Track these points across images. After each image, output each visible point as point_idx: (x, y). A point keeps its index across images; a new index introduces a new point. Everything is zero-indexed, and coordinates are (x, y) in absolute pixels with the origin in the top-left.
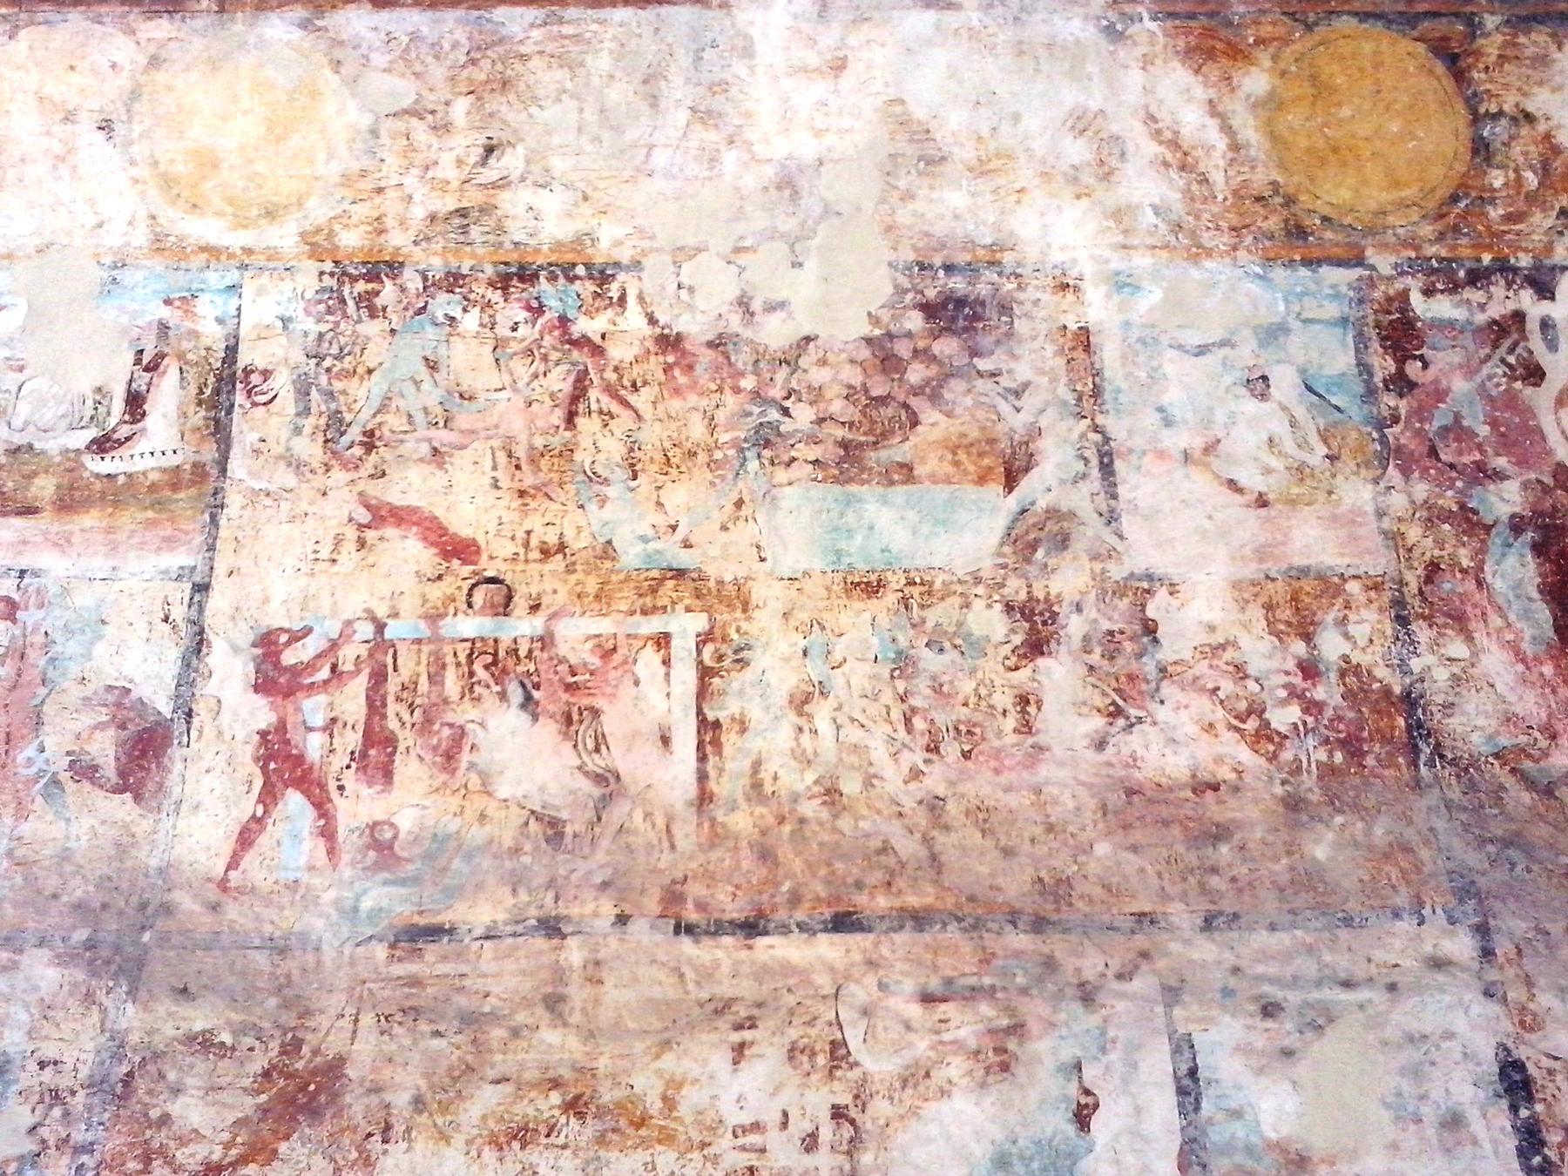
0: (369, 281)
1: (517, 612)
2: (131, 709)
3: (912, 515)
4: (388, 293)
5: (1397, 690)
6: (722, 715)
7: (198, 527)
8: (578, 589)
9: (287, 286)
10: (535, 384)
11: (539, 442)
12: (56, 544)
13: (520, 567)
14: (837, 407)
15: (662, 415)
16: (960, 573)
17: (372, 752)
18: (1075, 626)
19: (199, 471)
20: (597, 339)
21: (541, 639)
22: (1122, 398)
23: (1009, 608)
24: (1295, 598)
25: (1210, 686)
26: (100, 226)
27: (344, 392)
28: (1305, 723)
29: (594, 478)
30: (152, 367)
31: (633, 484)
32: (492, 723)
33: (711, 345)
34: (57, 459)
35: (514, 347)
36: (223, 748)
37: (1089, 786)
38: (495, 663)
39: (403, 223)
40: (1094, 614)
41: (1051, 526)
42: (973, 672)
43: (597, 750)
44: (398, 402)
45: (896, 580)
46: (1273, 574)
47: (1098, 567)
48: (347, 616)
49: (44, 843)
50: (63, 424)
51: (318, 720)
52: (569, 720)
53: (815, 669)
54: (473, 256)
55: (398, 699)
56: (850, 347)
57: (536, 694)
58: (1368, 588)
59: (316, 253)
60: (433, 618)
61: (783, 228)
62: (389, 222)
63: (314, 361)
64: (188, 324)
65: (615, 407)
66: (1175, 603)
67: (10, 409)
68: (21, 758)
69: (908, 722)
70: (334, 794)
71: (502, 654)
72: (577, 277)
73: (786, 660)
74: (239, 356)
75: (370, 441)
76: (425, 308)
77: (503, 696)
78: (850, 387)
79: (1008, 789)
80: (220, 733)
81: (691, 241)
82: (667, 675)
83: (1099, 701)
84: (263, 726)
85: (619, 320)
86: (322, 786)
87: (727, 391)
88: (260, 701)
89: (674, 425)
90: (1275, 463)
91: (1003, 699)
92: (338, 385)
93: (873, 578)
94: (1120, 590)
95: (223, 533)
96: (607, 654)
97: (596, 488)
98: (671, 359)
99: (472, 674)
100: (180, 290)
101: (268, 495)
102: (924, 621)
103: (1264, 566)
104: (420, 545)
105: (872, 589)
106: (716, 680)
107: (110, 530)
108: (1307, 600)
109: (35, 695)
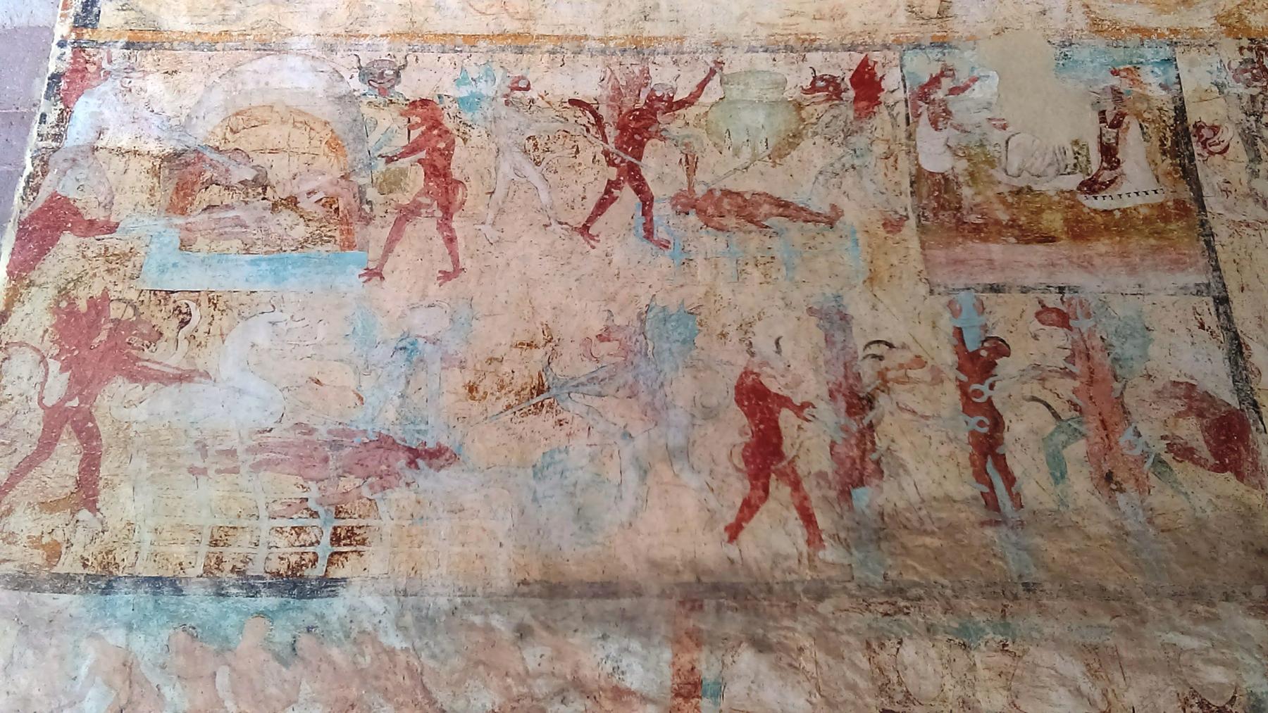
2: (1202, 400)
7: (1199, 252)
12: (1080, 266)
26: (1044, 13)
30: (1116, 124)
34: (1057, 198)
49: (1176, 513)
50: (1051, 171)
59: (1232, 31)
63: (1253, 118)
67: (1003, 159)
68: (1122, 441)
74: (1188, 115)
95: (1222, 256)
100: (1124, 63)
101: (1248, 226)
107: (1123, 255)
109: (1112, 389)
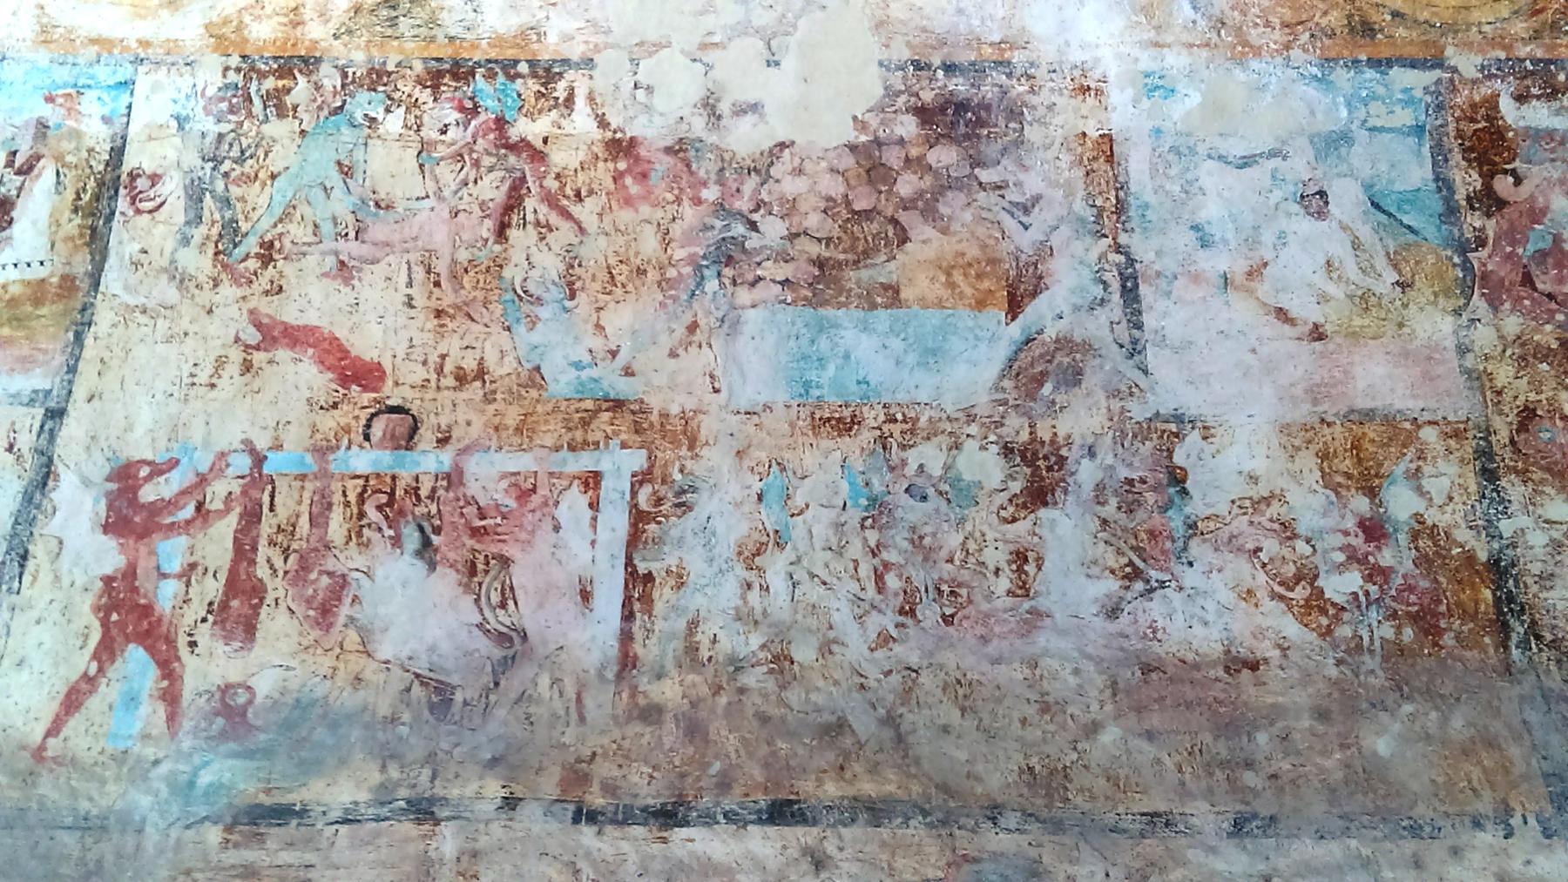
0: (281, 77)
1: (421, 446)
3: (896, 344)
4: (301, 89)
5: (1483, 556)
6: (656, 567)
7: (59, 346)
8: (497, 420)
9: (185, 82)
10: (465, 191)
11: (463, 256)
13: (430, 395)
14: (813, 221)
15: (608, 228)
16: (950, 409)
17: (235, 603)
18: (1086, 473)
19: (68, 283)
20: (539, 144)
21: (448, 476)
22: (1150, 215)
23: (1007, 450)
24: (1356, 446)
25: (1250, 546)
27: (242, 199)
28: (1367, 594)
29: (526, 296)
31: (568, 304)
32: (379, 573)
33: (668, 150)
35: (442, 151)
36: (59, 595)
37: (1098, 661)
38: (390, 504)
39: (323, 15)
40: (1110, 460)
41: (1063, 359)
42: (961, 521)
43: (503, 605)
44: (303, 209)
45: (873, 416)
46: (1330, 419)
47: (1116, 405)
48: (222, 446)
51: (175, 565)
52: (473, 571)
53: (770, 517)
54: (401, 51)
55: (272, 543)
56: (831, 154)
57: (436, 540)
58: (1447, 436)
60: (323, 451)
61: (757, 22)
62: (308, 14)
63: (211, 164)
64: (71, 123)
65: (555, 219)
66: (1211, 449)
69: (879, 579)
70: (184, 651)
71: (399, 493)
72: (519, 75)
73: (738, 505)
75: (268, 251)
76: (342, 107)
77: (397, 541)
78: (829, 199)
79: (997, 661)
80: (57, 578)
81: (652, 36)
82: (595, 519)
83: (1112, 561)
84: (108, 570)
85: (564, 123)
86: (171, 642)
87: (686, 203)
88: (110, 543)
89: (621, 240)
90: (1332, 289)
91: (995, 556)
92: (235, 191)
93: (847, 413)
94: (1143, 432)
96: (524, 495)
97: (526, 308)
98: (622, 165)
99: (362, 515)
100: (65, 85)
101: (144, 312)
102: (904, 463)
103: (1320, 409)
104: (314, 369)
105: (846, 425)
106: (652, 527)
108: (1372, 449)
